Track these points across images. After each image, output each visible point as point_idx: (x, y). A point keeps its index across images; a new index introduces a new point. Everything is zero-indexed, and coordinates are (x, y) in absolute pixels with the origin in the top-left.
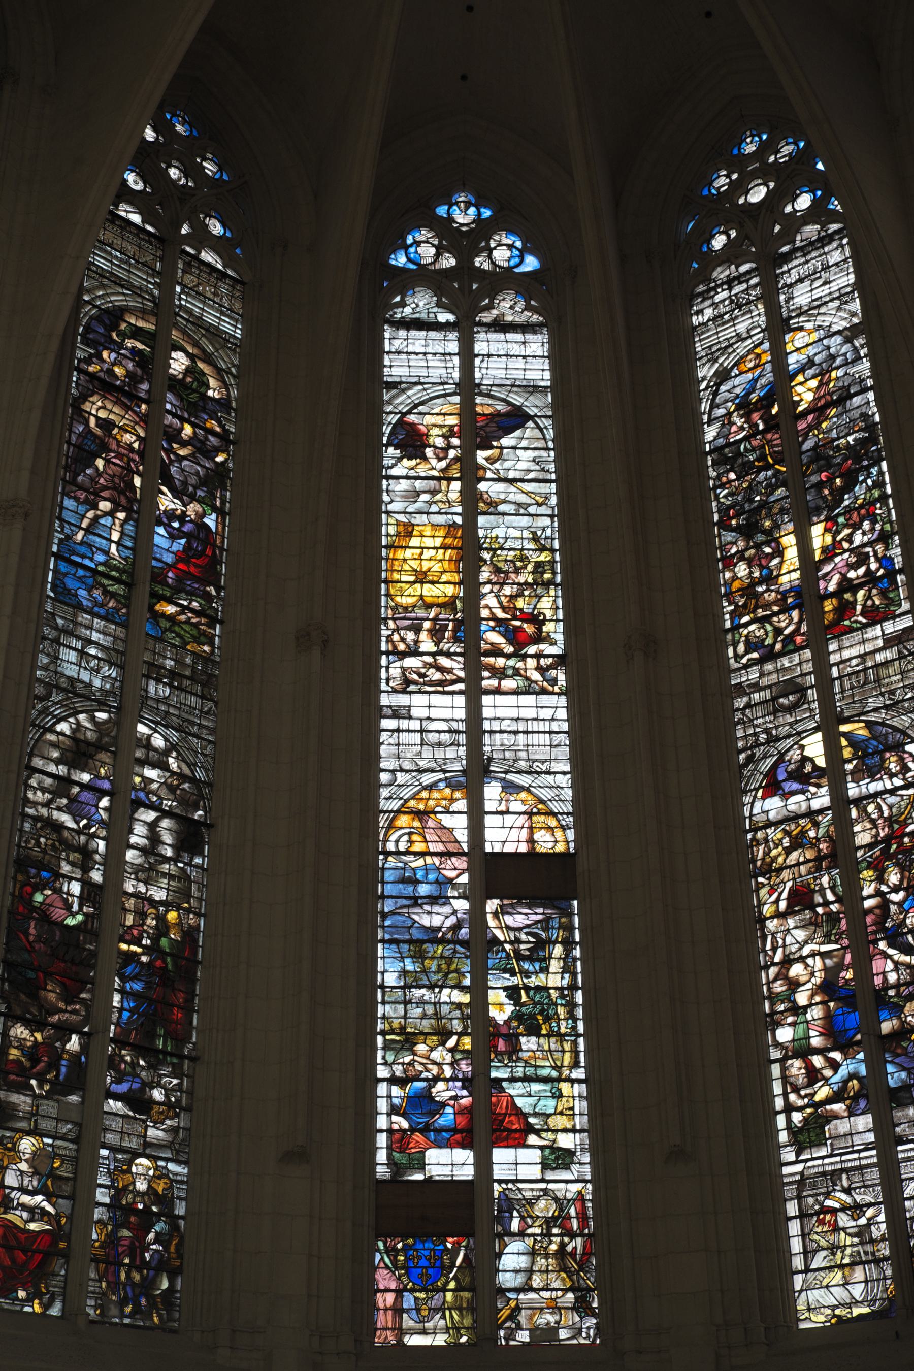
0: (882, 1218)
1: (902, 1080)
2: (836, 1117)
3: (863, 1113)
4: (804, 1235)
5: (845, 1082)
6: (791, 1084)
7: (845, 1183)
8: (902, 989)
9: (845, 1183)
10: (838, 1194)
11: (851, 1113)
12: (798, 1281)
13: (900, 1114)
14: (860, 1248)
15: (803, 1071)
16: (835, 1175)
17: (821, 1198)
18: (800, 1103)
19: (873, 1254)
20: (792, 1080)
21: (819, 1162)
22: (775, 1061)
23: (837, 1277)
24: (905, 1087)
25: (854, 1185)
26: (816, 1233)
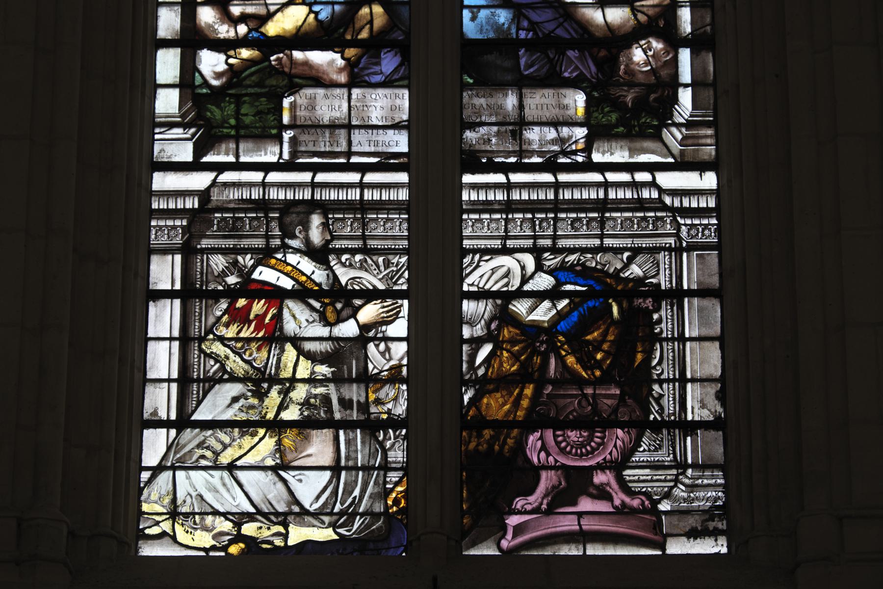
0: (399, 328)
1: (498, 28)
2: (316, 79)
3: (388, 83)
4: (185, 339)
7: (316, 236)
9: (316, 236)
10: (292, 259)
11: (357, 78)
12: (155, 445)
13: (481, 101)
14: (331, 390)
16: (292, 214)
17: (248, 260)
18: (225, 31)
19: (364, 407)
21: (256, 176)
23: (264, 448)
24: (500, 44)
25: (338, 244)
26: (222, 339)
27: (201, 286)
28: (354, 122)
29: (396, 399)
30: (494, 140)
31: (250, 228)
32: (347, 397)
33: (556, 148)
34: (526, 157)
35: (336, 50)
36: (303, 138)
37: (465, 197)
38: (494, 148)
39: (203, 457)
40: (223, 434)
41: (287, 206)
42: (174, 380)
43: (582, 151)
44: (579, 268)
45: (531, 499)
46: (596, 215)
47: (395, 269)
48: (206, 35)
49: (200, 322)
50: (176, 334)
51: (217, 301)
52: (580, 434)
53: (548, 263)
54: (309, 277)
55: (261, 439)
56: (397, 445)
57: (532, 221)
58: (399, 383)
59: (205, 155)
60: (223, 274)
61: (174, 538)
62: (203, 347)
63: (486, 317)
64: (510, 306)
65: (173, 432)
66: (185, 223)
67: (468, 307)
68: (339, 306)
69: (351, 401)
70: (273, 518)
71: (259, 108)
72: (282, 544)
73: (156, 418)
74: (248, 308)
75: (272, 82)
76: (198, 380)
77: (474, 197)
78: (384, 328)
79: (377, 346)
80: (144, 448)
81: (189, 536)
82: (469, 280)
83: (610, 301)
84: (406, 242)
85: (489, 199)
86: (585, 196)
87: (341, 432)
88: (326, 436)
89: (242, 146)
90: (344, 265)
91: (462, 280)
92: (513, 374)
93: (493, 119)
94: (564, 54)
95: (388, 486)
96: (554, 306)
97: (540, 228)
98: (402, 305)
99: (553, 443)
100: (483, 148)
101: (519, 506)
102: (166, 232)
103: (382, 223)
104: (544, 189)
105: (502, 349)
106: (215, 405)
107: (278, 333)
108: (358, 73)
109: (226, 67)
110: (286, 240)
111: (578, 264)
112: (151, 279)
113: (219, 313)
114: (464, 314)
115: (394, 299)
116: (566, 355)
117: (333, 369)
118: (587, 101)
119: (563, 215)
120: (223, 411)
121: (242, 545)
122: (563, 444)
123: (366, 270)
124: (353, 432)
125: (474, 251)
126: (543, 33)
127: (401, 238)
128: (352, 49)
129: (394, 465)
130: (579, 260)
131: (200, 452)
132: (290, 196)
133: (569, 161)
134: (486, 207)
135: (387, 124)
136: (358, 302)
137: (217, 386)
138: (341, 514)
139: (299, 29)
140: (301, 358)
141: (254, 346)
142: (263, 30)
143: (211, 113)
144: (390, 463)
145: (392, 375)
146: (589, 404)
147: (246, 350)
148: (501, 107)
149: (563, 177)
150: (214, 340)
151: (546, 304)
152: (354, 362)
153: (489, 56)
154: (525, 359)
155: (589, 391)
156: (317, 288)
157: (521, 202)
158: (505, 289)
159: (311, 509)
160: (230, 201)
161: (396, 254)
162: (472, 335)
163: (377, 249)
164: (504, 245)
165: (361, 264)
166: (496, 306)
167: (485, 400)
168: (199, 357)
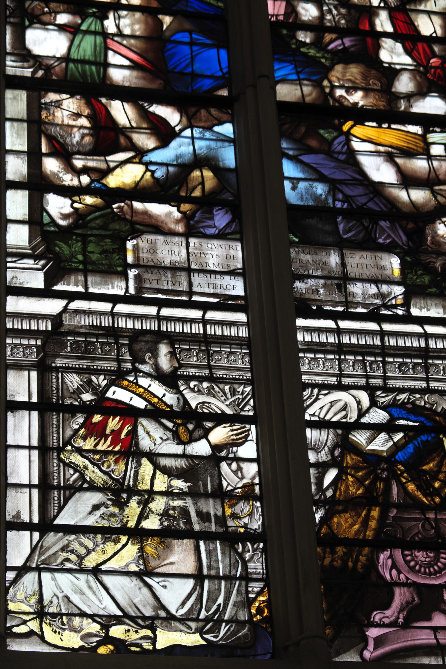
0: (249, 450)
1: (317, 198)
2: (156, 227)
3: (221, 236)
4: (44, 449)
5: (184, 168)
6: (51, 139)
7: (165, 363)
8: (328, 37)
10: (144, 382)
12: (19, 547)
13: (307, 257)
15: (83, 121)
16: (142, 342)
18: (68, 180)
19: (221, 521)
20: (53, 131)
21: (106, 307)
22: (16, 83)
23: (128, 555)
25: (185, 371)
26: (80, 451)
27: (58, 400)
28: (193, 267)
29: (251, 514)
30: (322, 291)
31: (102, 352)
32: (204, 511)
33: (378, 301)
34: (352, 307)
35: (173, 204)
36: (146, 276)
37: (300, 338)
38: (322, 298)
39: (67, 560)
40: (87, 540)
41: (136, 335)
42: (35, 486)
43: (401, 305)
44: (409, 406)
45: (388, 613)
46: (420, 361)
47: (241, 397)
48: (51, 182)
49: (58, 433)
50: (35, 443)
51: (74, 416)
52: (427, 554)
53: (381, 400)
54: (160, 400)
55: (124, 546)
56: (256, 558)
57: (363, 362)
58: (253, 500)
59: (56, 284)
60: (78, 392)
61: (42, 637)
62: (62, 457)
63: (329, 444)
64: (350, 436)
65: (36, 535)
66: (39, 343)
67: (311, 434)
68: (191, 427)
69: (208, 514)
70: (140, 621)
71: (105, 247)
72: (151, 648)
73: (19, 521)
74: (104, 423)
75: (116, 226)
76: (59, 488)
77: (308, 338)
78: (235, 449)
79: (229, 465)
80: (8, 548)
81: (57, 636)
82: (310, 411)
83: (441, 436)
84: (249, 374)
85: (322, 341)
86: (408, 344)
87: (202, 543)
88: (187, 546)
89: (90, 279)
90: (192, 390)
91: (305, 410)
92: (359, 497)
93: (320, 273)
94: (377, 224)
95: (250, 595)
96: (391, 438)
97: (371, 369)
98: (250, 430)
99: (402, 562)
100: (313, 297)
101: (377, 619)
102: (21, 350)
103: (225, 356)
104: (371, 336)
105: (347, 474)
106: (76, 512)
107: (133, 449)
108: (193, 225)
109: (72, 210)
110: (137, 365)
111: (408, 402)
112: (8, 391)
113: (76, 427)
114: (309, 441)
115: (242, 424)
116: (406, 483)
117: (189, 484)
118: (401, 264)
119: (391, 360)
120: (85, 518)
121: (111, 647)
122: (412, 563)
123: (214, 396)
124: (213, 543)
125: (313, 386)
126: (357, 205)
127: (244, 370)
128: (187, 205)
129: (254, 576)
130: (409, 399)
131: (64, 555)
132: (138, 326)
133: (390, 313)
134: (319, 348)
135: (223, 270)
136: (209, 424)
137: (77, 495)
138: (207, 620)
139: (137, 184)
140: (158, 472)
141: (112, 459)
142: (104, 181)
143: (60, 248)
144: (251, 573)
145: (246, 492)
146: (432, 528)
147: (104, 462)
148: (325, 263)
149: (387, 327)
150: (72, 451)
151: (383, 436)
152: (209, 478)
153: (310, 220)
154: (370, 483)
155: (431, 516)
156: (169, 409)
157: (350, 345)
158: (344, 420)
159: (178, 615)
160: (82, 327)
161: (241, 384)
162: (318, 460)
163: (222, 378)
164: (340, 382)
165: (209, 391)
166: (337, 435)
167: (335, 520)
168: (59, 466)
